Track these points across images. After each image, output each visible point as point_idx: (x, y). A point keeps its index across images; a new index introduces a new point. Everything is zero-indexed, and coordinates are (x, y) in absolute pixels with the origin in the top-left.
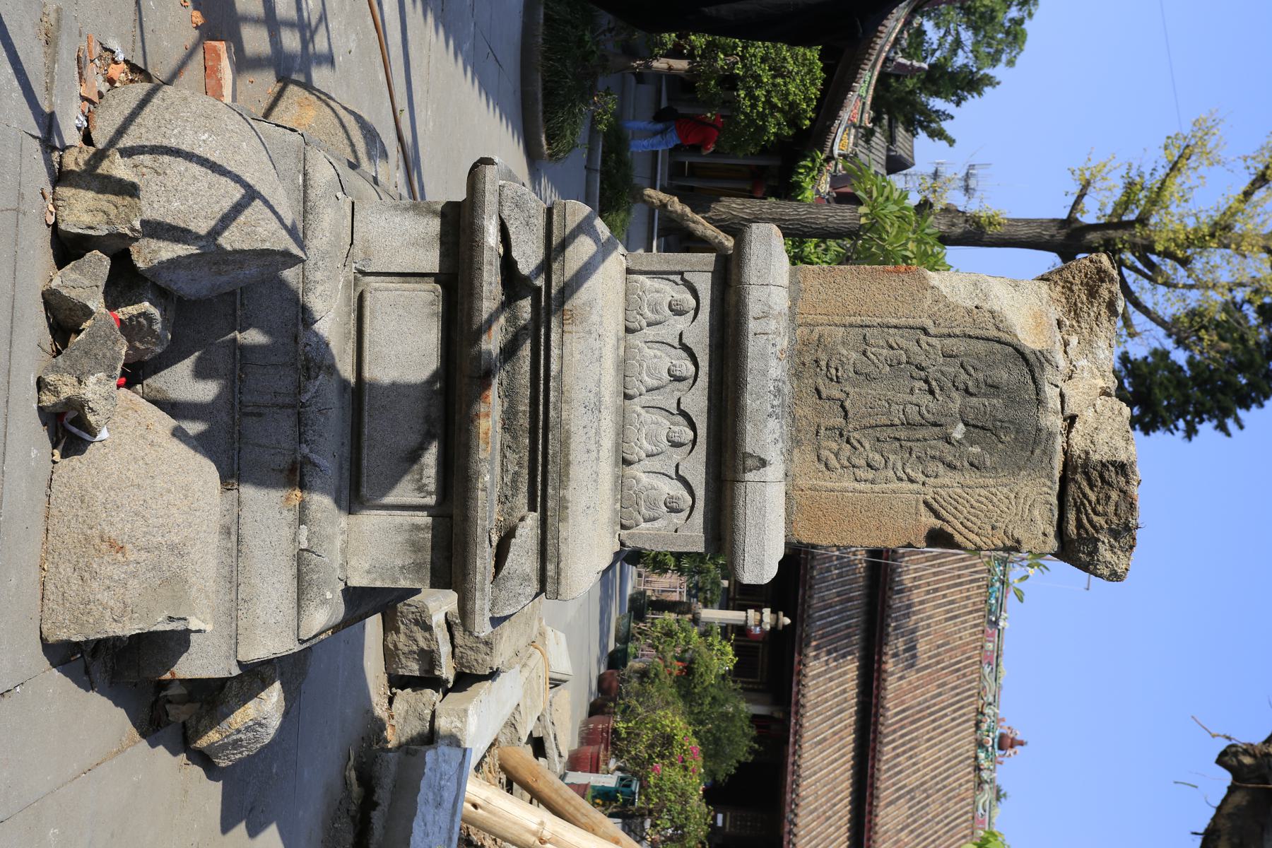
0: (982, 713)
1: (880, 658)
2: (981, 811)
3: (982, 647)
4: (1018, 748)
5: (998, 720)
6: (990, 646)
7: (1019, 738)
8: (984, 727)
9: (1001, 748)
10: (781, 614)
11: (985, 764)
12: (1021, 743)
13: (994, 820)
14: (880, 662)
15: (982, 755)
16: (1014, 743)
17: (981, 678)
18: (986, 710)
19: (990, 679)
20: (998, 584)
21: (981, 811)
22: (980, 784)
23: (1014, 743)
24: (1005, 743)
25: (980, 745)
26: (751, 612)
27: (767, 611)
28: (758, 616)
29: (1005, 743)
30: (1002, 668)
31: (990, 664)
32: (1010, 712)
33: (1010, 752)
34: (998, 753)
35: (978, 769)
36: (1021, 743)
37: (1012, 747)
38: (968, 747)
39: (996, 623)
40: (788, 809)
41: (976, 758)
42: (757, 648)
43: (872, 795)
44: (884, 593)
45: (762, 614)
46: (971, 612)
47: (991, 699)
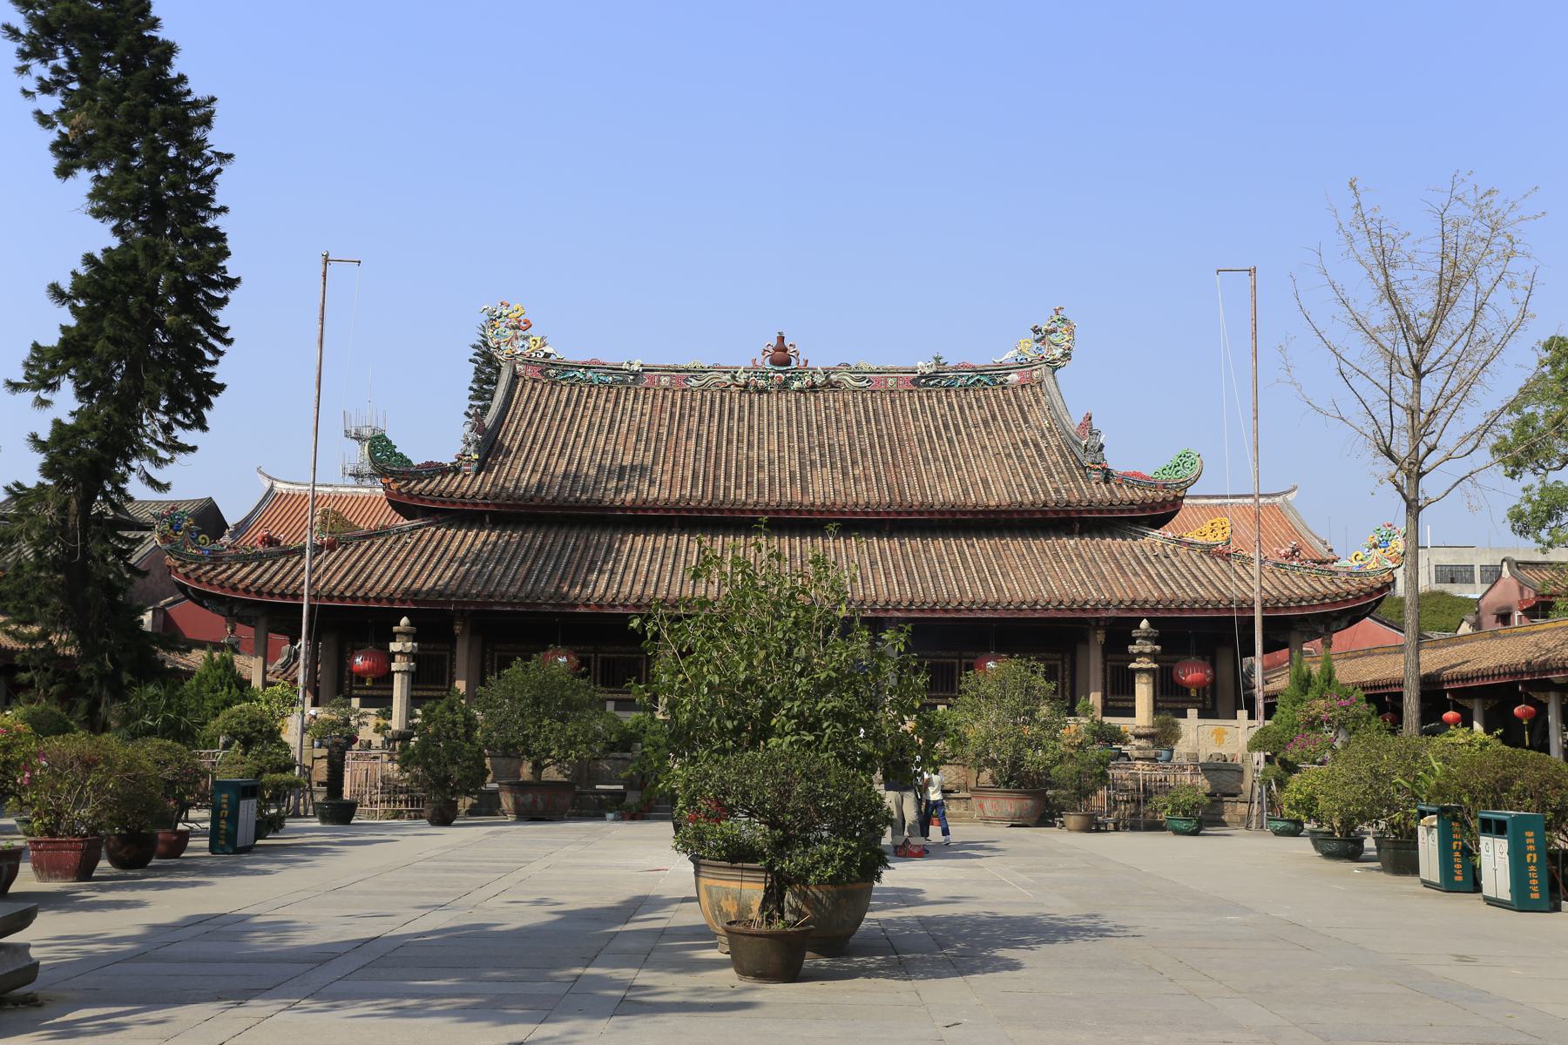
0: (746, 386)
1: (618, 508)
2: (864, 383)
3: (666, 389)
4: (787, 343)
5: (755, 370)
6: (665, 381)
7: (774, 343)
8: (762, 383)
9: (788, 363)
10: (395, 629)
12: (781, 339)
13: (874, 368)
14: (623, 508)
15: (797, 384)
16: (781, 347)
17: (703, 389)
18: (742, 381)
19: (706, 378)
20: (589, 374)
21: (864, 383)
22: (832, 386)
23: (781, 347)
24: (781, 356)
25: (784, 386)
26: (394, 667)
27: (395, 647)
28: (398, 657)
29: (781, 356)
30: (689, 364)
31: (686, 380)
32: (744, 353)
34: (794, 364)
35: (813, 387)
36: (781, 339)
38: (784, 402)
39: (636, 374)
41: (800, 390)
42: (603, 659)
43: (788, 511)
44: (538, 506)
45: (394, 654)
46: (616, 404)
47: (728, 376)
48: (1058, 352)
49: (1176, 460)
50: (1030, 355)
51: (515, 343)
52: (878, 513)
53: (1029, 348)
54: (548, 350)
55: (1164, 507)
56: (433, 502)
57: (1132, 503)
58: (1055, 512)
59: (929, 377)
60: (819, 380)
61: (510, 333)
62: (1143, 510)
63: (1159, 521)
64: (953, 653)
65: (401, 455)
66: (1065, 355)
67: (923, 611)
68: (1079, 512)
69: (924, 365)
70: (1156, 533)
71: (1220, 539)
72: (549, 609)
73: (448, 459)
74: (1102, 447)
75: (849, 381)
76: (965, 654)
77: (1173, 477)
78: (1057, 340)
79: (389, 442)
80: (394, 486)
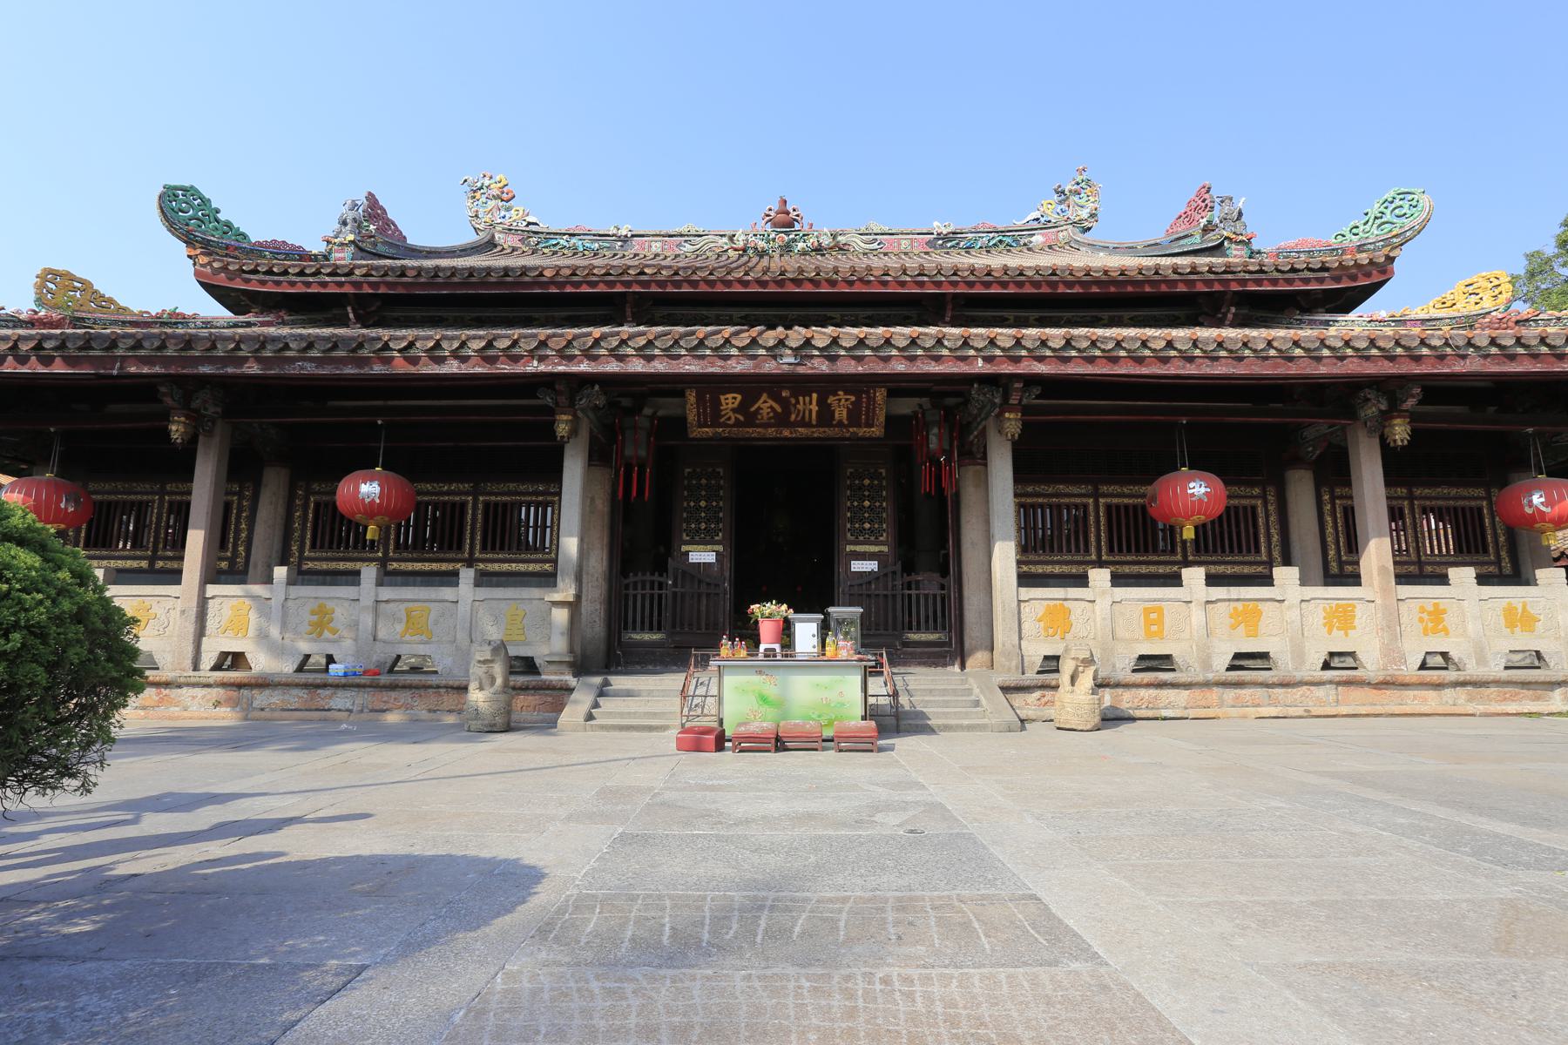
2: (875, 246)
7: (776, 207)
8: (761, 244)
11: (812, 241)
13: (886, 229)
15: (801, 245)
18: (741, 244)
20: (574, 240)
21: (875, 246)
25: (787, 249)
29: (785, 221)
30: (684, 230)
31: (679, 245)
33: (793, 214)
34: (797, 226)
37: (788, 213)
39: (625, 240)
40: (770, 367)
47: (725, 240)
48: (1084, 214)
49: (1375, 210)
50: (1054, 218)
51: (496, 214)
52: (938, 284)
53: (1050, 209)
54: (531, 219)
55: (1368, 275)
56: (263, 283)
57: (1324, 269)
58: (1208, 282)
59: (945, 238)
60: (826, 241)
61: (492, 203)
62: (1337, 279)
63: (1346, 300)
64: (1083, 489)
65: (228, 225)
66: (1092, 215)
67: (1091, 360)
68: (1243, 282)
69: (938, 226)
70: (1352, 316)
71: (1487, 304)
72: (310, 369)
73: (317, 247)
74: (1240, 214)
75: (858, 243)
76: (1104, 489)
77: (1375, 233)
78: (1082, 202)
79: (205, 202)
80: (203, 260)
